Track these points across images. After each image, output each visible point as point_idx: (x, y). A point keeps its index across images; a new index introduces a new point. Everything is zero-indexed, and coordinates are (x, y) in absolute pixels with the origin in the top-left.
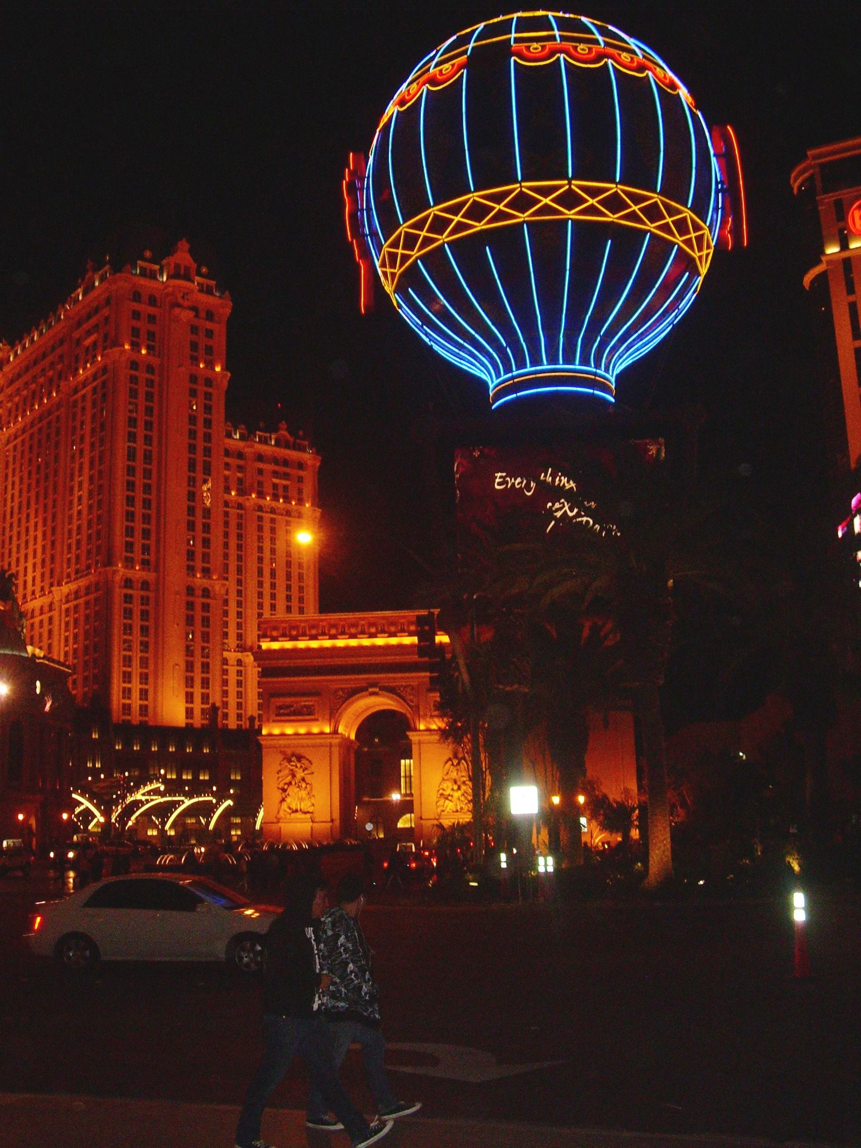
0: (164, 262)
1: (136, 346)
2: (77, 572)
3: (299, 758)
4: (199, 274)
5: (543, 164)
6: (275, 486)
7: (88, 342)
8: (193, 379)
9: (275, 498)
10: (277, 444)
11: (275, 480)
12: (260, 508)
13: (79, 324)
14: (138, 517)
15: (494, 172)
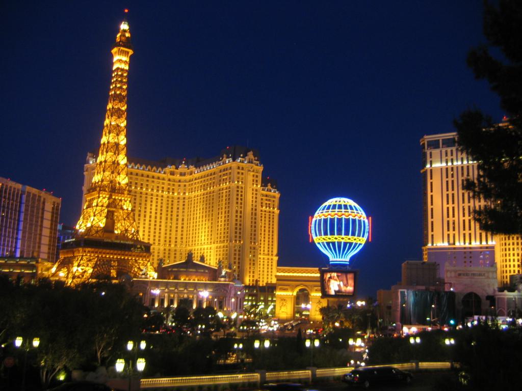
0: (246, 157)
1: (238, 181)
2: (220, 241)
3: (284, 300)
4: (255, 160)
5: (339, 233)
6: (266, 204)
7: (225, 177)
8: (253, 190)
9: (266, 207)
10: (267, 191)
11: (266, 202)
12: (262, 211)
13: (221, 171)
14: (238, 229)
15: (332, 233)
